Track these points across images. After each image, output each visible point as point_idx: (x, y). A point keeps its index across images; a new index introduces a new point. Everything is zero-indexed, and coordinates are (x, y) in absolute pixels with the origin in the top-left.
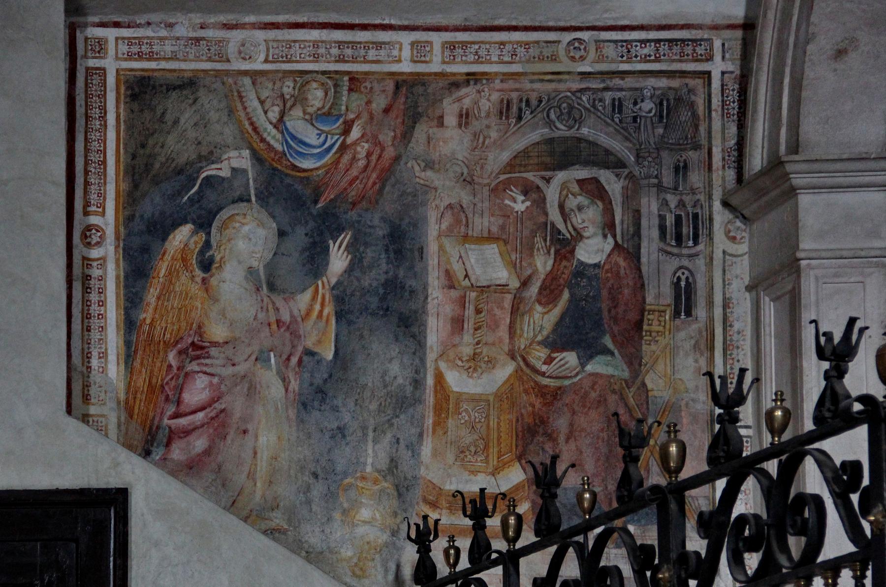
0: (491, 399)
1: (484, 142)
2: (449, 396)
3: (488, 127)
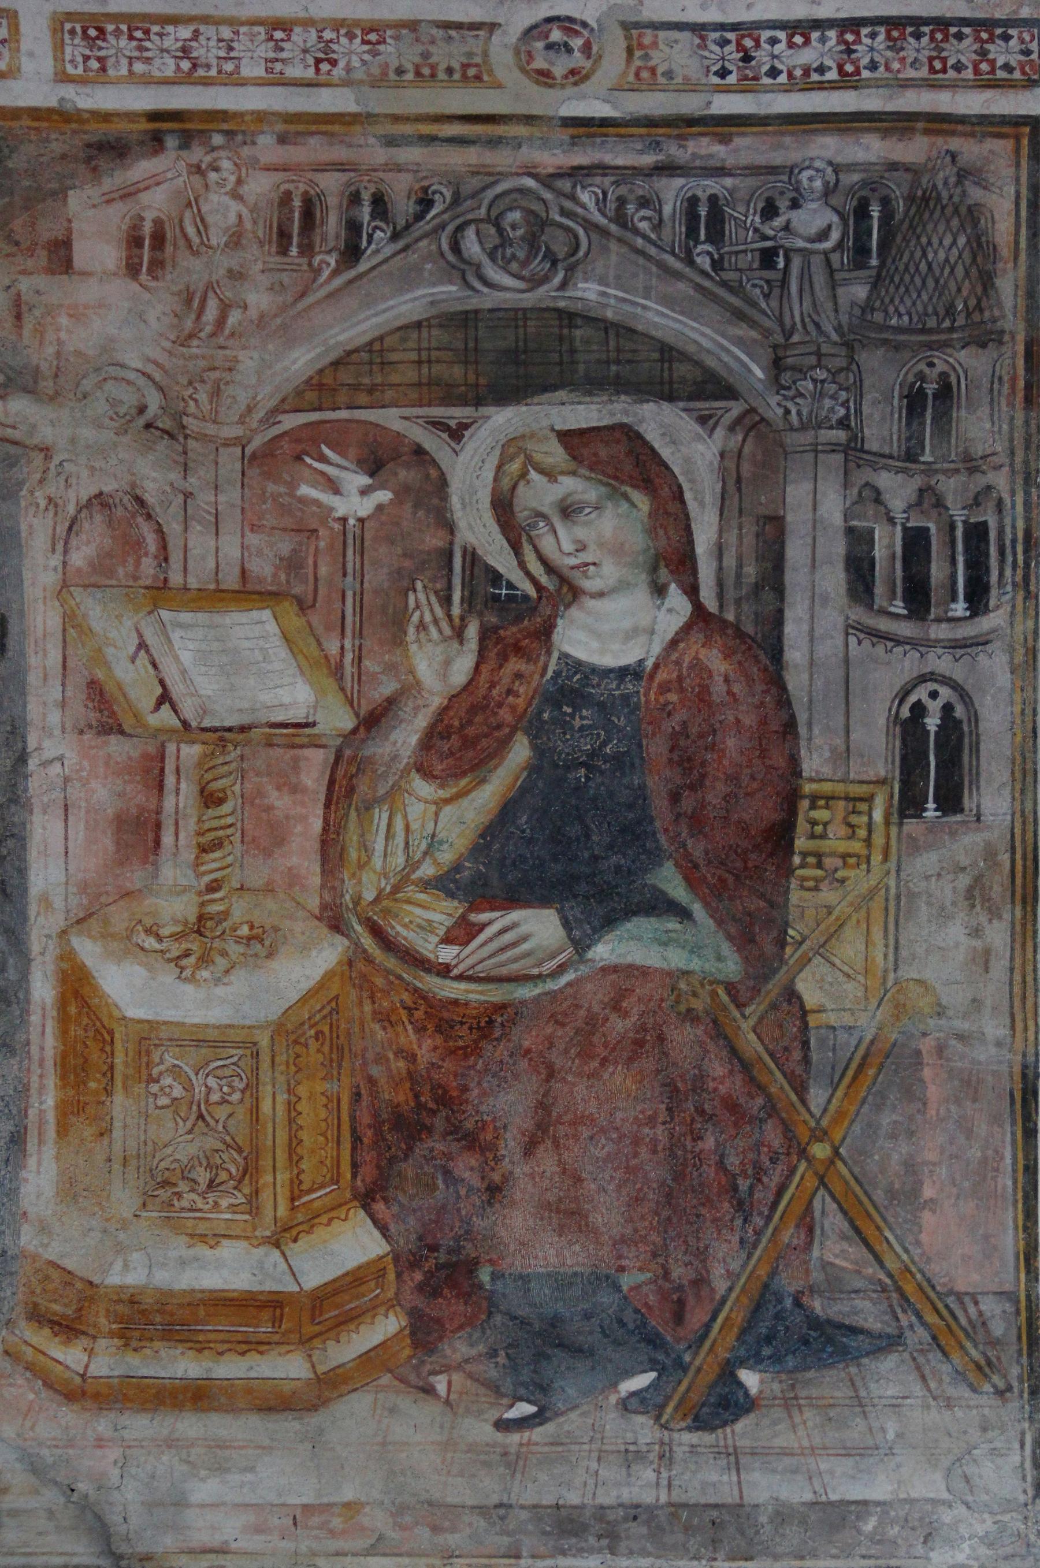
0: (264, 1041)
1: (221, 322)
2: (111, 1033)
3: (236, 276)
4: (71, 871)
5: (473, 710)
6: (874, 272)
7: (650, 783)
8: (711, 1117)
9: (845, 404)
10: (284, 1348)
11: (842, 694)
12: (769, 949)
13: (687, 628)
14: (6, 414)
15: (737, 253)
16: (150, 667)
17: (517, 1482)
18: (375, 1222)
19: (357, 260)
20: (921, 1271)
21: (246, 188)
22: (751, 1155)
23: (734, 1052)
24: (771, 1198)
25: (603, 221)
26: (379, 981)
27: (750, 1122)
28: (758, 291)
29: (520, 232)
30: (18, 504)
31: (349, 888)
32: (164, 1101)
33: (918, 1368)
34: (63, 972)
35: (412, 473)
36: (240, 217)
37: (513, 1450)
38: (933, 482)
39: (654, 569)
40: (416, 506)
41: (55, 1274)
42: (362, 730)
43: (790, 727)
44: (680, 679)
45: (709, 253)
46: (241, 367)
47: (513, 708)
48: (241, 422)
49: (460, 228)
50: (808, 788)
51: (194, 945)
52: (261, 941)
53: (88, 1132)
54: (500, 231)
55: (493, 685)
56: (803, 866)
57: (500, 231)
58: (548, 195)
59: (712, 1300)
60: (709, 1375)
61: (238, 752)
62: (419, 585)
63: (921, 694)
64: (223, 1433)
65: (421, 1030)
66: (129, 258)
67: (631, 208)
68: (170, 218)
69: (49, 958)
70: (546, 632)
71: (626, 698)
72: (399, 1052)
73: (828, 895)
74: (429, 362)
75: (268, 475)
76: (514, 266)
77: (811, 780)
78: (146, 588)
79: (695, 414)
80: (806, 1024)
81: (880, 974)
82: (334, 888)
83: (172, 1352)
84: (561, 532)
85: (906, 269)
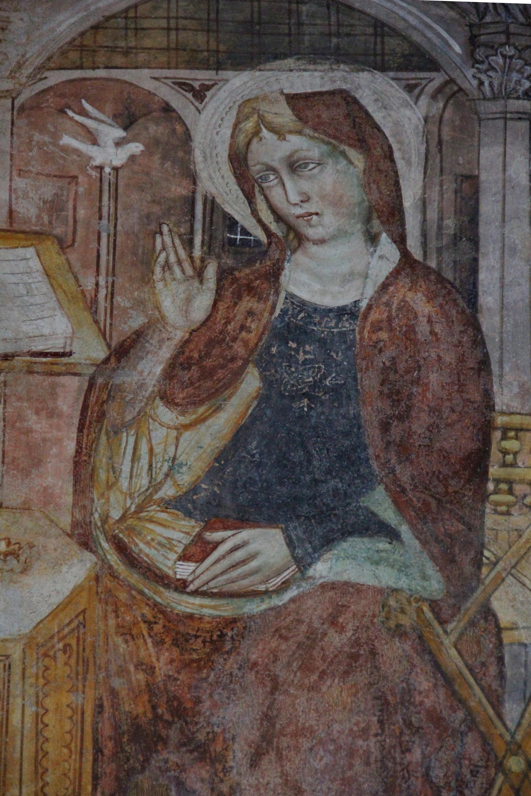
5: (211, 343)
8: (417, 731)
12: (468, 569)
13: (396, 273)
22: (453, 768)
23: (437, 666)
26: (123, 596)
27: (453, 735)
31: (98, 504)
35: (161, 129)
39: (368, 220)
40: (165, 158)
42: (113, 360)
44: (390, 319)
46: (12, 27)
47: (246, 343)
48: (12, 76)
50: (500, 420)
52: (17, 557)
55: (228, 322)
56: (496, 492)
62: (165, 229)
65: (159, 643)
71: (343, 335)
72: (139, 665)
74: (177, 29)
77: (503, 413)
79: (404, 83)
82: (84, 507)
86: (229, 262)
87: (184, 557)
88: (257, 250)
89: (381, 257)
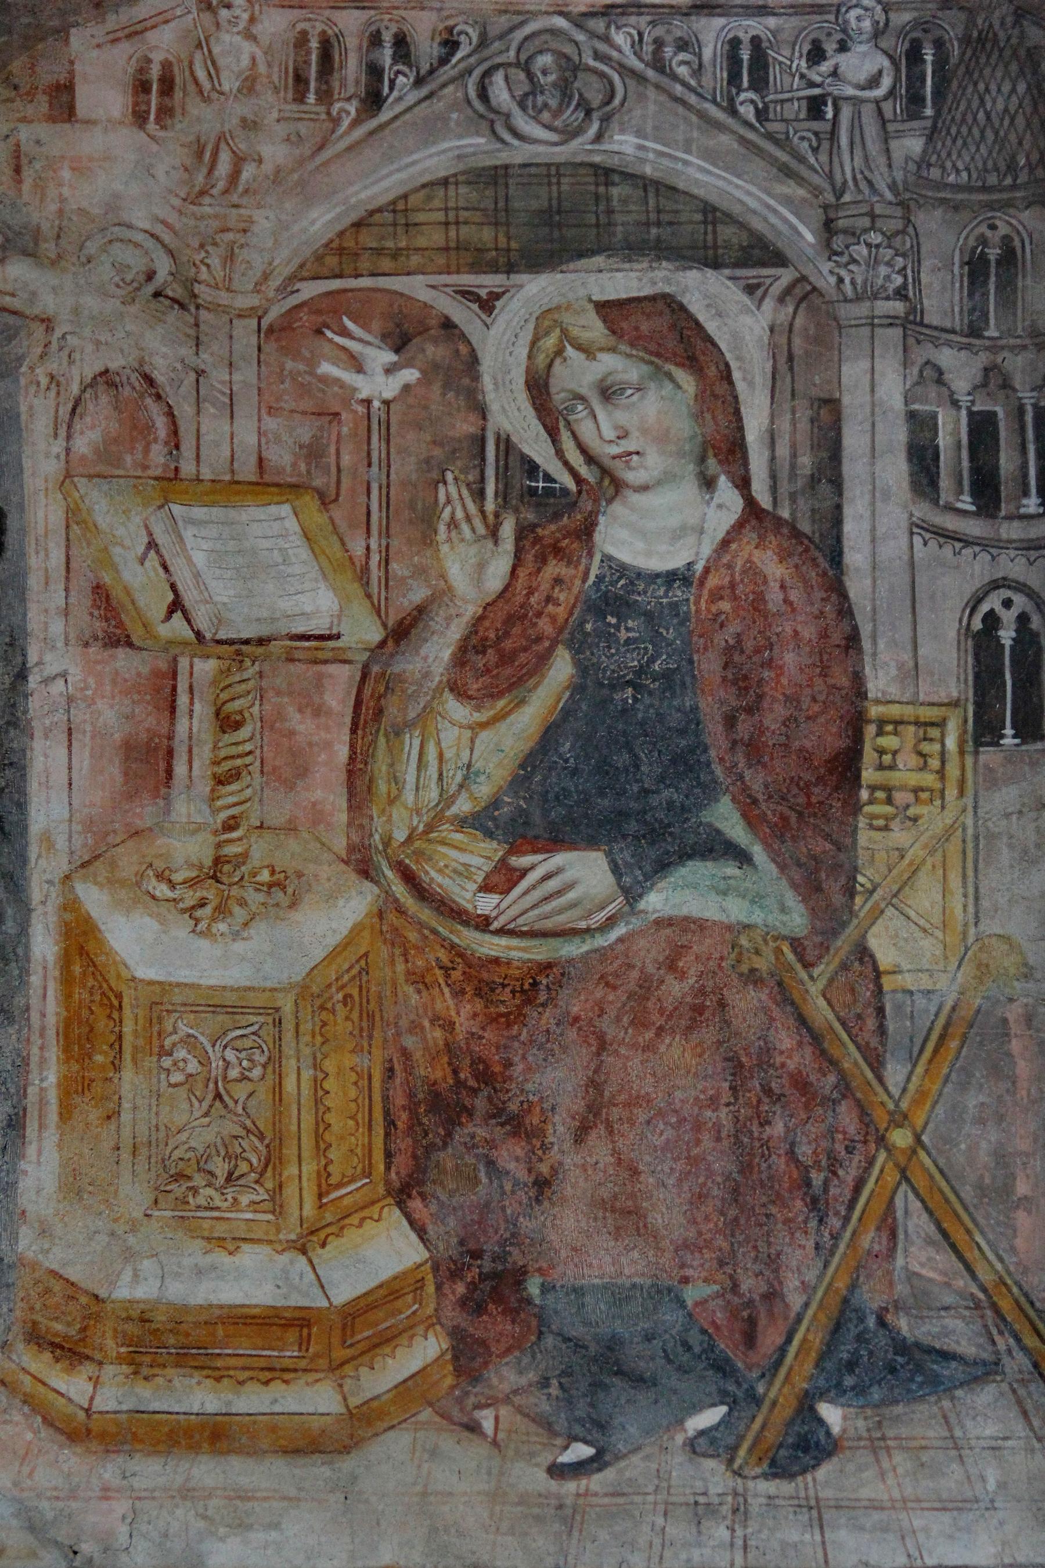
2: (119, 996)
4: (75, 805)
5: (510, 620)
6: (928, 123)
7: (702, 705)
8: (779, 1097)
9: (902, 271)
10: (311, 1377)
11: (908, 603)
12: (838, 899)
13: (739, 526)
14: (5, 280)
15: (782, 101)
16: (161, 570)
17: (574, 1542)
18: (411, 1223)
19: (379, 108)
20: (1017, 1283)
21: (260, 27)
22: (824, 1144)
23: (802, 1020)
24: (848, 1195)
25: (638, 65)
26: (413, 936)
27: (822, 1105)
28: (805, 144)
29: (552, 78)
30: (17, 381)
31: (379, 824)
32: (177, 1077)
33: (1019, 1402)
34: (66, 924)
36: (253, 59)
37: (568, 1502)
38: (999, 360)
39: (702, 459)
40: (446, 386)
41: (57, 1287)
42: (390, 643)
43: (853, 640)
44: (733, 586)
45: (752, 101)
46: (256, 229)
47: (553, 619)
49: (488, 73)
51: (210, 892)
52: (284, 889)
53: (94, 1115)
54: (530, 76)
55: (531, 592)
56: (871, 802)
57: (530, 76)
58: (581, 37)
59: (786, 1318)
60: (786, 1410)
61: (257, 667)
62: (449, 476)
63: (993, 602)
64: (244, 1481)
65: (458, 993)
66: (136, 104)
67: (668, 51)
68: (180, 61)
69: (50, 908)
70: (586, 531)
71: (674, 606)
72: (435, 1020)
73: (899, 836)
74: (457, 223)
75: (285, 351)
76: (546, 116)
77: (877, 702)
78: (156, 479)
79: (743, 282)
80: (879, 990)
81: (960, 928)
82: (361, 826)
83: (187, 1381)
84: (601, 416)
85: (963, 120)
86: (530, 516)
87: (486, 888)
88: (563, 501)
89: (720, 506)
